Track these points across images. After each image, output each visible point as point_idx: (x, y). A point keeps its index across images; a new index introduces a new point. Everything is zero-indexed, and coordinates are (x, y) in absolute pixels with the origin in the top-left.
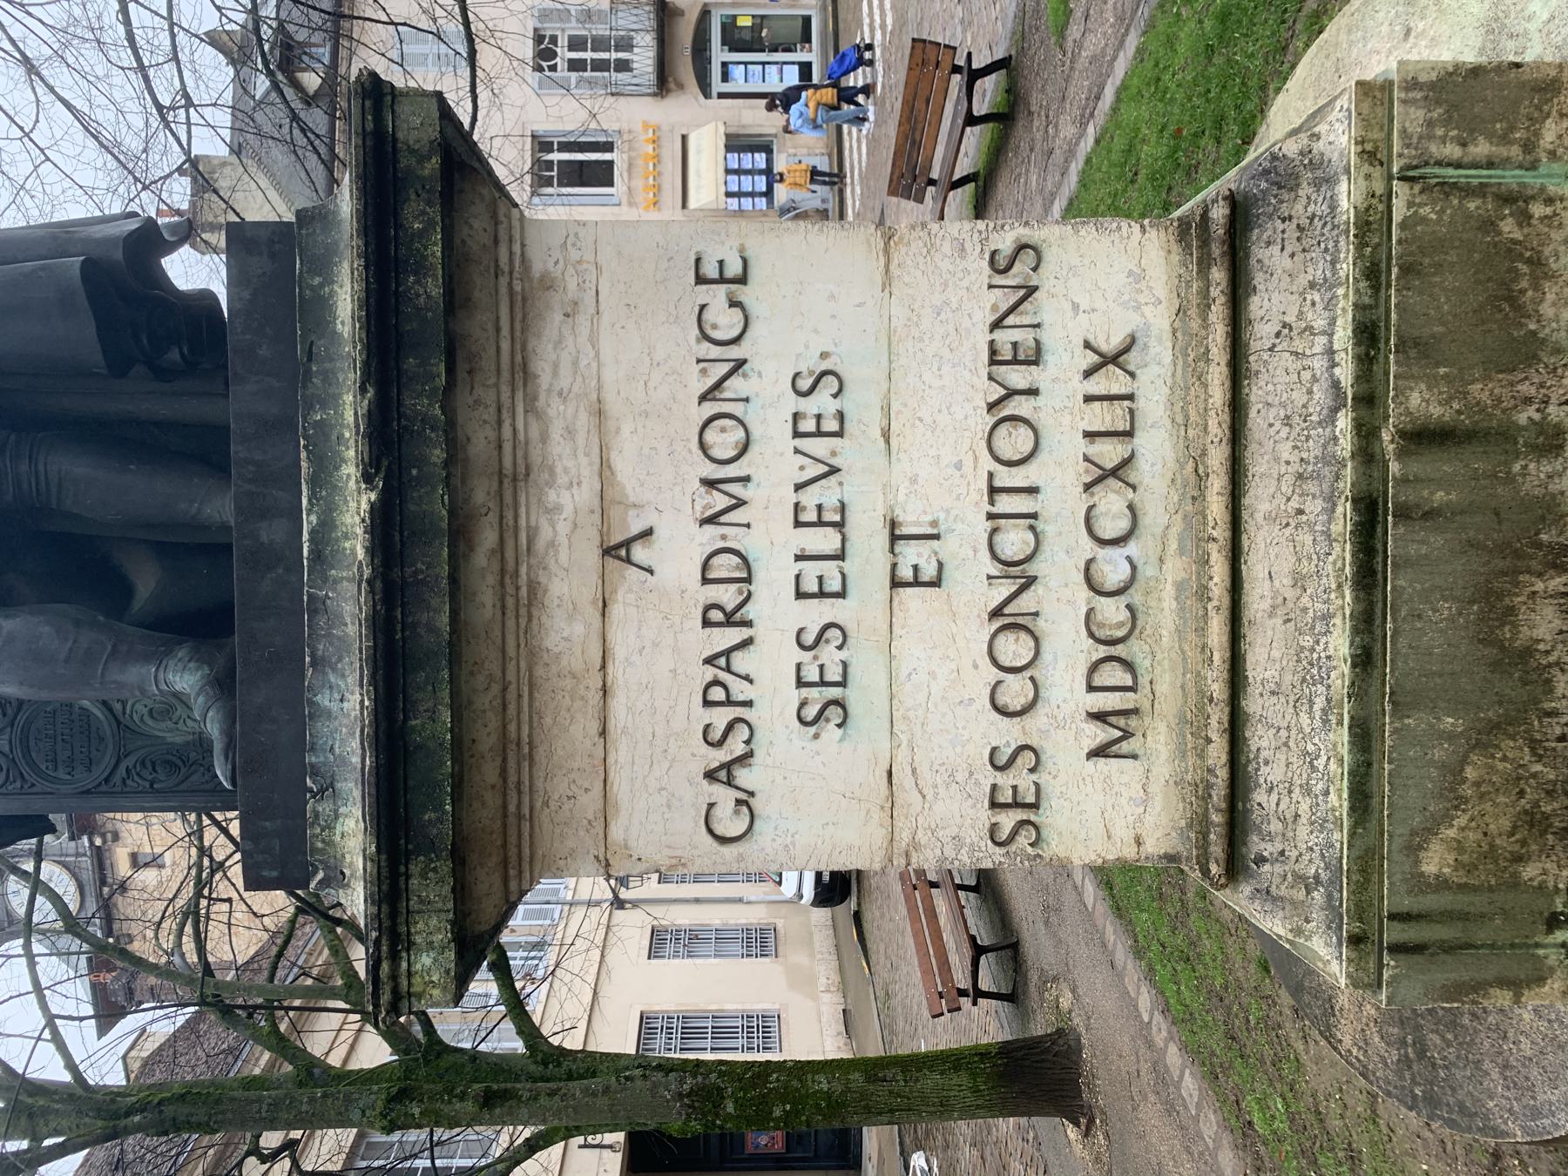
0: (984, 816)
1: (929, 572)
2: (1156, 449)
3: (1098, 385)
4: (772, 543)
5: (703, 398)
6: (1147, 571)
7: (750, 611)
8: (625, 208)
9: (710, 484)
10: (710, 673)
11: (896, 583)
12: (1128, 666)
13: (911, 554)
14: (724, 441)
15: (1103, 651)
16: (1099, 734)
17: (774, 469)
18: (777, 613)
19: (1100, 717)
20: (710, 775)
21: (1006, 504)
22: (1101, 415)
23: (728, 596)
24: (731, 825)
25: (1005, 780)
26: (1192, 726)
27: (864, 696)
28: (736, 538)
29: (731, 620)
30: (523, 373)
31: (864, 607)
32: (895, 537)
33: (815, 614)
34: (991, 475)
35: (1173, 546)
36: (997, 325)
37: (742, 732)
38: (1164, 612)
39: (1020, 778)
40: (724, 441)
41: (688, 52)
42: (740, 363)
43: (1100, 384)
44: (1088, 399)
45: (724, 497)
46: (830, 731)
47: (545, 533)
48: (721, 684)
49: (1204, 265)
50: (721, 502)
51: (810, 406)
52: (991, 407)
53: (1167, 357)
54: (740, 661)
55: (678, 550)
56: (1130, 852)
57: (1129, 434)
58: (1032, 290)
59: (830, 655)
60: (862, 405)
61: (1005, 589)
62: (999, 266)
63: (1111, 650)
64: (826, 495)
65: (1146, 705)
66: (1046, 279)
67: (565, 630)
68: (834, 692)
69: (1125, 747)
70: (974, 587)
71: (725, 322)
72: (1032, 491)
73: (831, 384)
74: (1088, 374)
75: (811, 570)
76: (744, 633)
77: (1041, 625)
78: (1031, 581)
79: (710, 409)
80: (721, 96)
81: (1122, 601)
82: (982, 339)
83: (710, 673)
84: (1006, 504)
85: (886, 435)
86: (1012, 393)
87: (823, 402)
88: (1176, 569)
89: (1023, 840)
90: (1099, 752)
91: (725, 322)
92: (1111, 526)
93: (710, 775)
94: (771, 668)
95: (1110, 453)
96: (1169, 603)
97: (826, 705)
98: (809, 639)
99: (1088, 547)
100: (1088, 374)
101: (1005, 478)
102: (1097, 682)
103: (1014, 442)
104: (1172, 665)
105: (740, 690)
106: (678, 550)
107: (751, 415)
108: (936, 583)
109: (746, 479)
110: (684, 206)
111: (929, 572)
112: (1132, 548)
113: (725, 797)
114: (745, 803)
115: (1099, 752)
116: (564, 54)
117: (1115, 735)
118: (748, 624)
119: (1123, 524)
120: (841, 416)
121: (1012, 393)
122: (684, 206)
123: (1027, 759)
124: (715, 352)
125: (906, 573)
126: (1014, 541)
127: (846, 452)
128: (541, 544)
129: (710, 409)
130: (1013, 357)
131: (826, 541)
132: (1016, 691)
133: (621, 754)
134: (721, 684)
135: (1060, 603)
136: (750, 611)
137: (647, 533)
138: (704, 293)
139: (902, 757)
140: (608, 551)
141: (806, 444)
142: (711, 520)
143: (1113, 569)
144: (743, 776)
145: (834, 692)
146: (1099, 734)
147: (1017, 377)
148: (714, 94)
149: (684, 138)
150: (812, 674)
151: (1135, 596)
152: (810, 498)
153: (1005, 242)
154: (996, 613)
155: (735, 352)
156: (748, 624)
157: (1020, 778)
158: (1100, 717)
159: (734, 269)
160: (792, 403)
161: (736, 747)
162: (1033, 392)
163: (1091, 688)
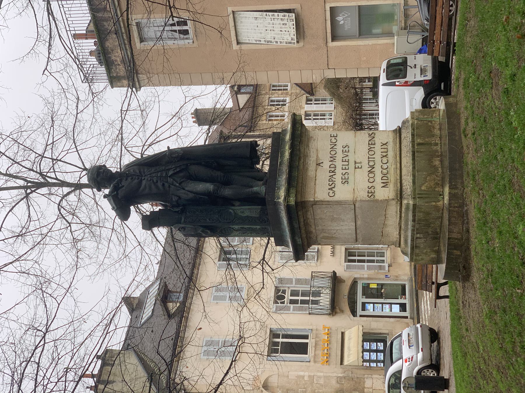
0: (367, 194)
1: (360, 167)
2: (391, 154)
3: (383, 147)
4: (339, 163)
6: (390, 167)
8: (312, 363)
11: (355, 168)
12: (387, 177)
13: (357, 165)
14: (333, 153)
16: (383, 185)
17: (340, 156)
18: (339, 171)
21: (370, 159)
23: (333, 169)
24: (331, 194)
26: (396, 184)
27: (351, 180)
28: (334, 163)
29: (333, 172)
30: (308, 146)
32: (355, 163)
33: (344, 172)
38: (392, 171)
40: (333, 153)
41: (346, 297)
43: (383, 147)
45: (333, 158)
46: (346, 184)
48: (331, 179)
49: (396, 135)
50: (332, 159)
51: (345, 149)
54: (334, 176)
55: (326, 164)
56: (387, 198)
59: (346, 176)
60: (351, 149)
61: (370, 169)
64: (347, 158)
66: (376, 136)
67: (311, 172)
70: (366, 168)
71: (334, 141)
75: (344, 167)
80: (361, 316)
84: (370, 159)
87: (346, 149)
88: (393, 166)
89: (372, 197)
94: (338, 178)
95: (384, 154)
96: (393, 170)
97: (345, 181)
99: (382, 164)
104: (392, 177)
105: (333, 180)
106: (326, 164)
107: (337, 150)
110: (342, 363)
111: (360, 167)
112: (387, 164)
113: (331, 192)
114: (334, 192)
116: (288, 297)
117: (385, 185)
122: (342, 363)
126: (371, 163)
127: (349, 154)
131: (347, 163)
132: (371, 180)
133: (317, 186)
134: (331, 179)
135: (378, 170)
139: (356, 187)
143: (385, 166)
144: (333, 189)
146: (383, 185)
147: (372, 146)
148: (358, 315)
149: (343, 334)
151: (388, 169)
152: (344, 159)
153: (371, 132)
159: (335, 135)
160: (342, 149)
161: (333, 186)
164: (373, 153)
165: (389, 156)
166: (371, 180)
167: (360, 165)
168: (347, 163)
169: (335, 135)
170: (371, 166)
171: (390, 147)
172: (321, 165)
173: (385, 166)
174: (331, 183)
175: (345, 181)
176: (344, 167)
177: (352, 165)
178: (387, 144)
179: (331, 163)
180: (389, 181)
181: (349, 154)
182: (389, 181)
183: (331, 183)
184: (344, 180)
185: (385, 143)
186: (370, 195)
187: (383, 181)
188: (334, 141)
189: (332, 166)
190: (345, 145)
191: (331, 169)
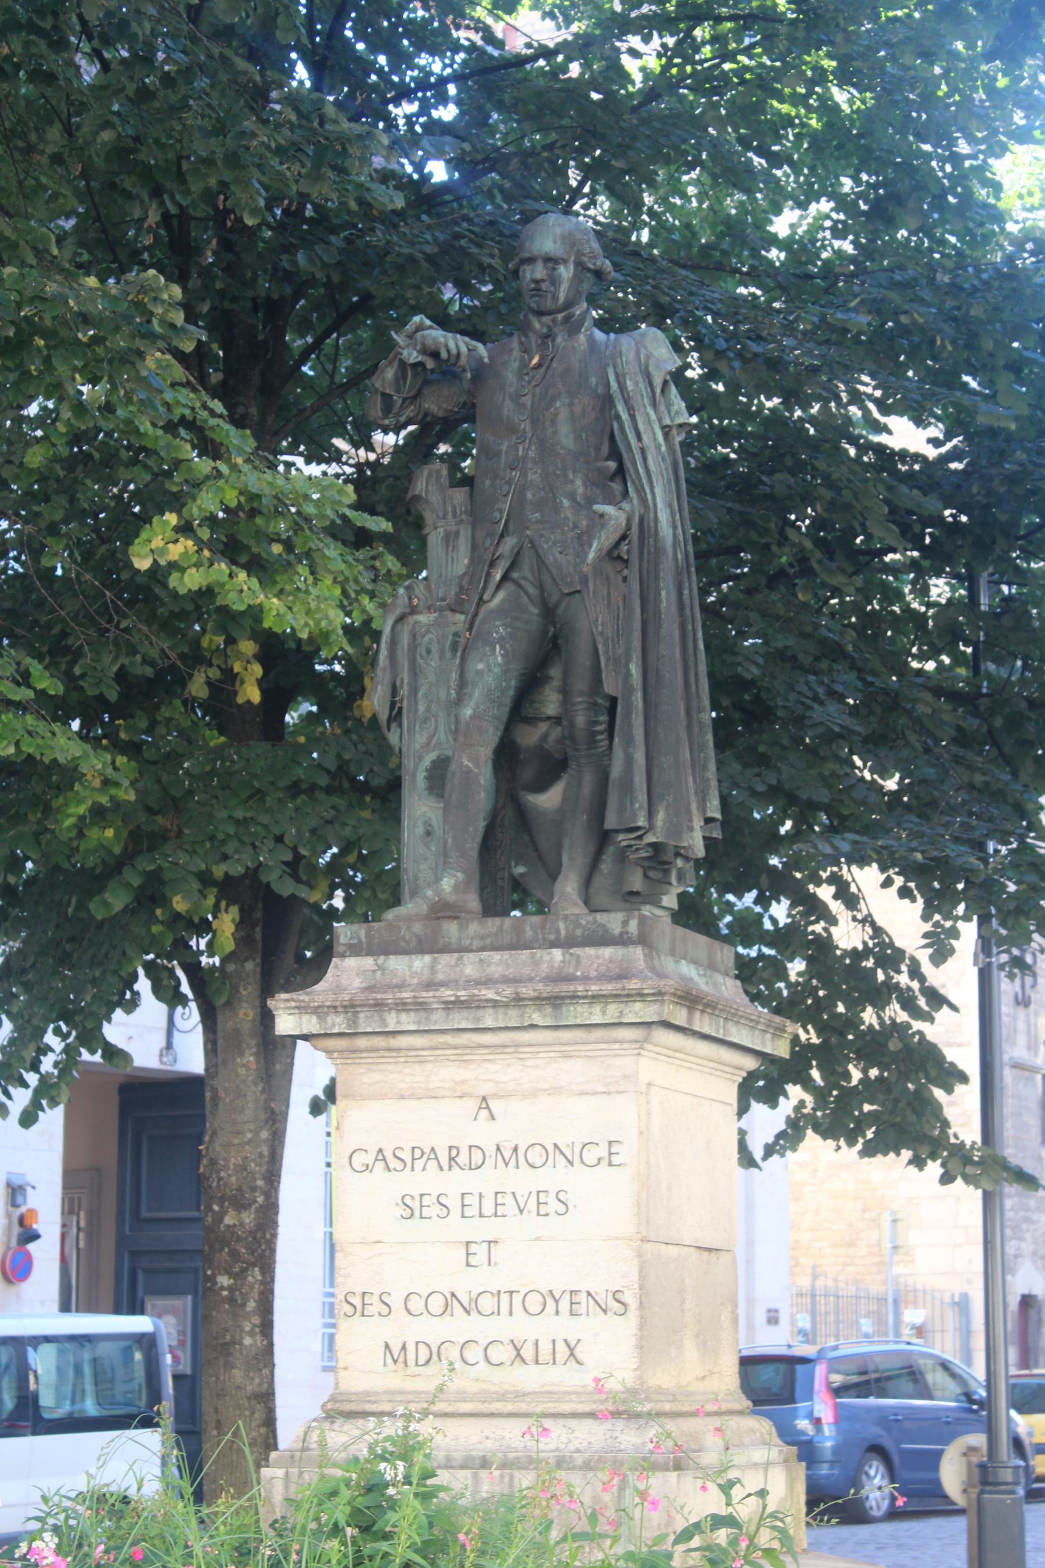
0: (359, 1290)
1: (473, 1260)
3: (561, 1347)
4: (488, 1180)
5: (556, 1146)
9: (515, 1149)
10: (427, 1150)
11: (468, 1243)
13: (481, 1251)
15: (435, 1350)
16: (396, 1349)
17: (522, 1181)
19: (404, 1348)
20: (380, 1151)
21: (505, 1298)
22: (545, 1349)
23: (463, 1159)
24: (358, 1161)
25: (376, 1298)
29: (451, 1159)
31: (458, 1228)
33: (453, 1202)
35: (484, 1386)
36: (589, 1294)
37: (400, 1166)
39: (376, 1307)
42: (571, 1163)
43: (561, 1347)
44: (511, 1313)
45: (511, 1156)
46: (400, 1210)
47: (493, 1067)
48: (423, 1155)
50: (507, 1156)
51: (552, 1200)
54: (433, 1164)
55: (485, 1134)
57: (537, 1362)
58: (605, 1311)
59: (436, 1209)
61: (465, 1302)
63: (435, 1354)
64: (510, 1208)
65: (409, 1371)
68: (417, 1213)
69: (389, 1360)
70: (466, 1284)
71: (590, 1157)
72: (511, 1313)
73: (562, 1209)
75: (473, 1200)
76: (445, 1166)
77: (446, 1317)
78: (468, 1312)
82: (584, 1287)
83: (427, 1150)
84: (505, 1298)
85: (537, 1239)
86: (557, 1301)
87: (554, 1206)
88: (475, 1388)
89: (349, 1309)
90: (387, 1346)
91: (590, 1157)
92: (494, 1354)
93: (380, 1151)
94: (428, 1180)
95: (528, 1352)
97: (411, 1209)
98: (442, 1200)
99: (484, 1342)
101: (517, 1299)
102: (421, 1346)
103: (534, 1303)
105: (419, 1164)
108: (468, 1265)
111: (473, 1260)
112: (483, 1364)
113: (369, 1159)
115: (387, 1346)
117: (396, 1355)
118: (450, 1168)
119: (494, 1361)
121: (557, 1301)
123: (385, 1310)
124: (577, 1151)
125: (473, 1248)
126: (487, 1303)
128: (487, 1065)
130: (572, 1301)
131: (488, 1208)
132: (416, 1304)
135: (458, 1327)
140: (484, 1099)
141: (534, 1195)
142: (498, 1149)
143: (474, 1354)
144: (380, 1165)
145: (417, 1213)
146: (396, 1349)
147: (564, 1305)
150: (426, 1201)
152: (509, 1200)
153: (629, 1298)
154: (453, 1295)
155: (576, 1160)
156: (450, 1168)
157: (376, 1307)
158: (404, 1348)
159: (615, 1160)
161: (393, 1163)
162: (557, 1313)
165: (519, 1370)
166: (416, 1304)
168: (488, 1210)
169: (615, 1160)
171: (563, 1377)
172: (484, 1113)
173: (474, 1354)
174: (406, 1155)
175: (411, 1209)
177: (481, 1230)
180: (412, 1369)
182: (412, 1369)
183: (406, 1155)
184: (415, 1206)
186: (356, 1301)
189: (477, 1157)
191: (464, 1152)
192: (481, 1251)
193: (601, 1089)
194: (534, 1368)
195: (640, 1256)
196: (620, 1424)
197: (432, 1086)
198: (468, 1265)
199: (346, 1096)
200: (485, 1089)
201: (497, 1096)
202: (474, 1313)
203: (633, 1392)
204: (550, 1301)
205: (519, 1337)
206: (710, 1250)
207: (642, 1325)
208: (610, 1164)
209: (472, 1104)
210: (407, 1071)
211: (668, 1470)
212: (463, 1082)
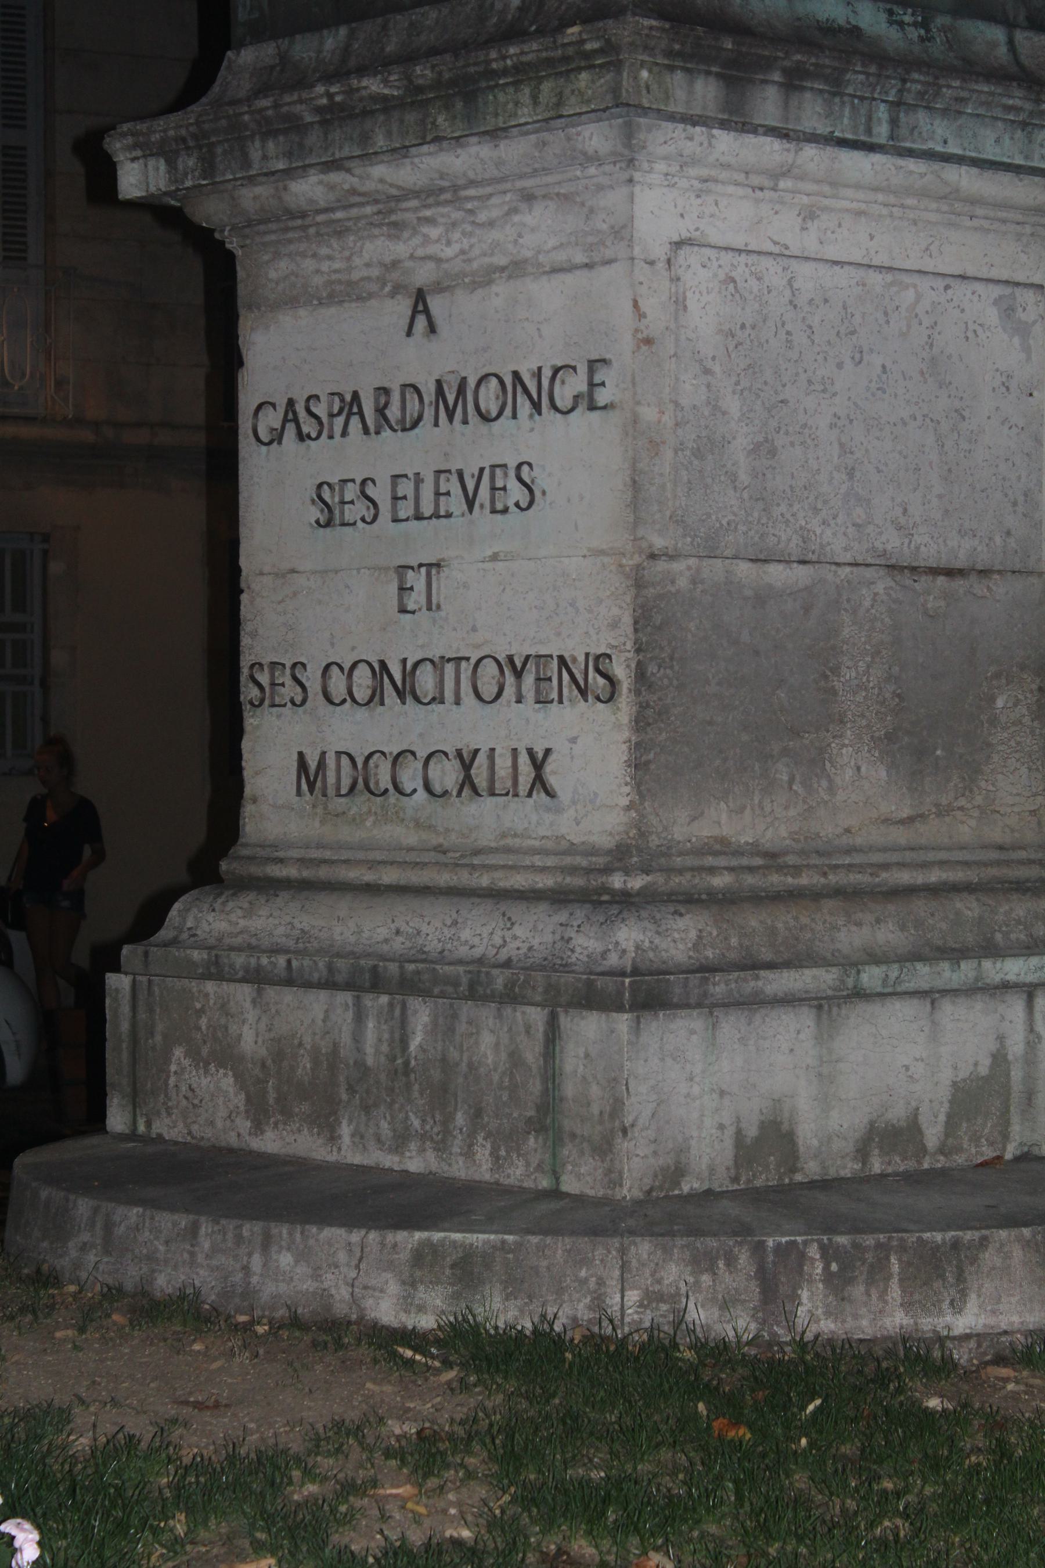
5: (516, 375)
7: (387, 433)
11: (402, 569)
16: (313, 765)
22: (503, 764)
23: (393, 412)
29: (381, 411)
33: (380, 493)
34: (468, 659)
36: (562, 659)
45: (452, 400)
46: (315, 513)
47: (434, 232)
51: (513, 484)
52: (510, 659)
53: (542, 832)
54: (355, 422)
55: (421, 363)
62: (600, 662)
64: (456, 503)
70: (401, 646)
71: (564, 395)
74: (530, 752)
79: (508, 380)
81: (391, 787)
85: (494, 557)
87: (516, 493)
95: (480, 772)
99: (422, 754)
100: (530, 752)
109: (465, 422)
112: (421, 795)
118: (377, 433)
120: (505, 511)
126: (426, 680)
129: (508, 380)
132: (338, 684)
136: (387, 433)
137: (432, 329)
138: (582, 369)
143: (410, 777)
146: (313, 765)
151: (393, 797)
153: (620, 671)
161: (309, 427)
163: (339, 753)
164: (488, 690)
167: (416, 599)
168: (427, 509)
169: (602, 397)
170: (410, 672)
172: (421, 322)
176: (406, 488)
178: (540, 796)
179: (429, 391)
181: (482, 517)
185: (552, 780)
187: (331, 762)
188: (564, 395)
190: (542, 481)
191: (396, 397)
192: (417, 580)
193: (580, 258)
194: (490, 802)
195: (639, 584)
196: (580, 913)
197: (356, 276)
198: (403, 610)
199: (250, 308)
200: (423, 275)
201: (439, 288)
202: (409, 699)
203: (620, 856)
204: (510, 679)
205: (469, 741)
206: (950, 573)
207: (640, 723)
208: (592, 407)
209: (403, 306)
210: (324, 251)
211: (620, 1009)
212: (395, 264)
